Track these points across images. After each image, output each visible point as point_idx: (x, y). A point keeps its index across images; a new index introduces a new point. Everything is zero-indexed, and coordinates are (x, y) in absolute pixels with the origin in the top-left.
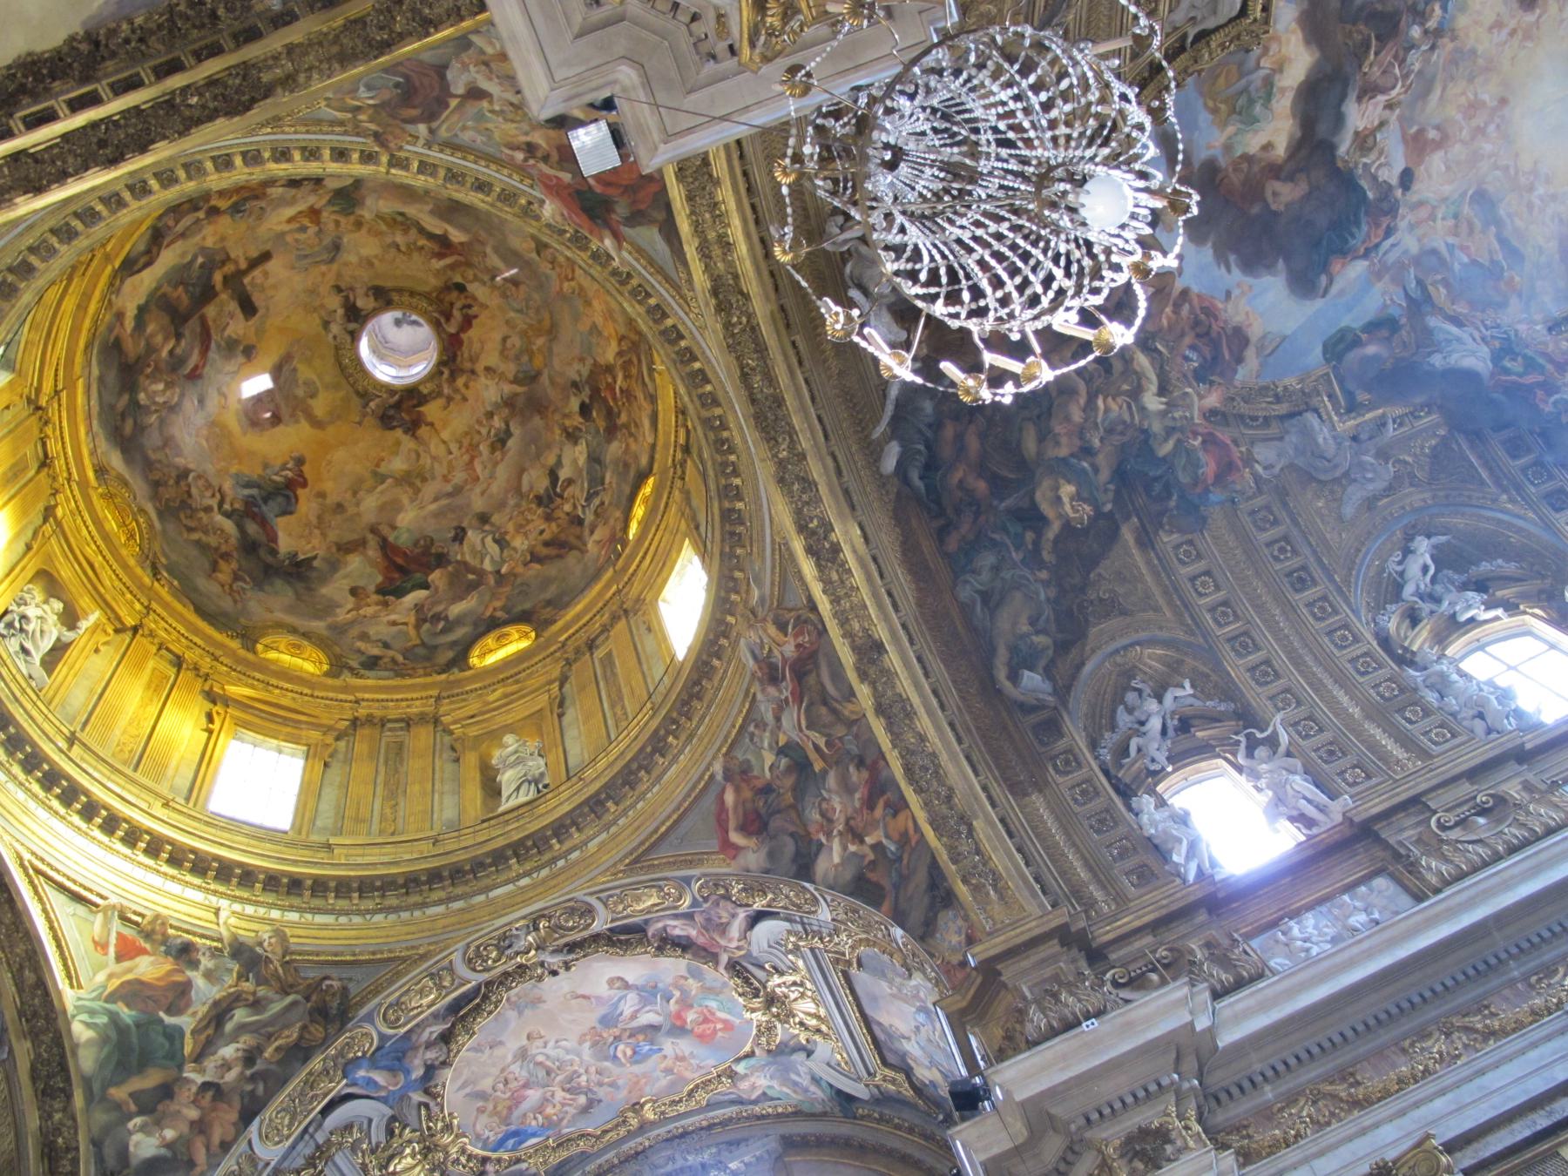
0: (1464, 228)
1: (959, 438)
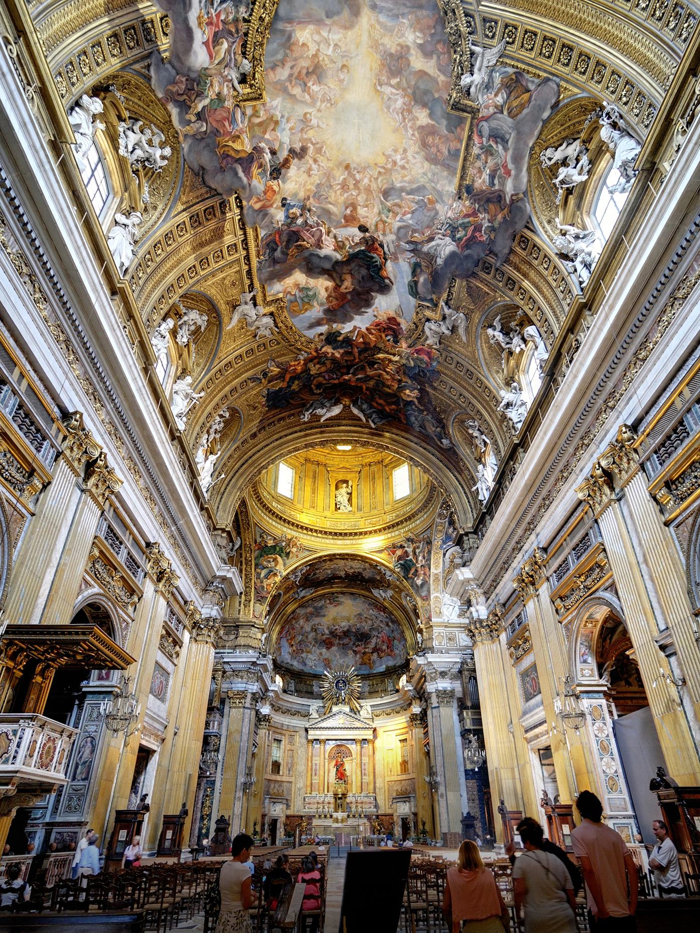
0: (396, 209)
1: (377, 403)
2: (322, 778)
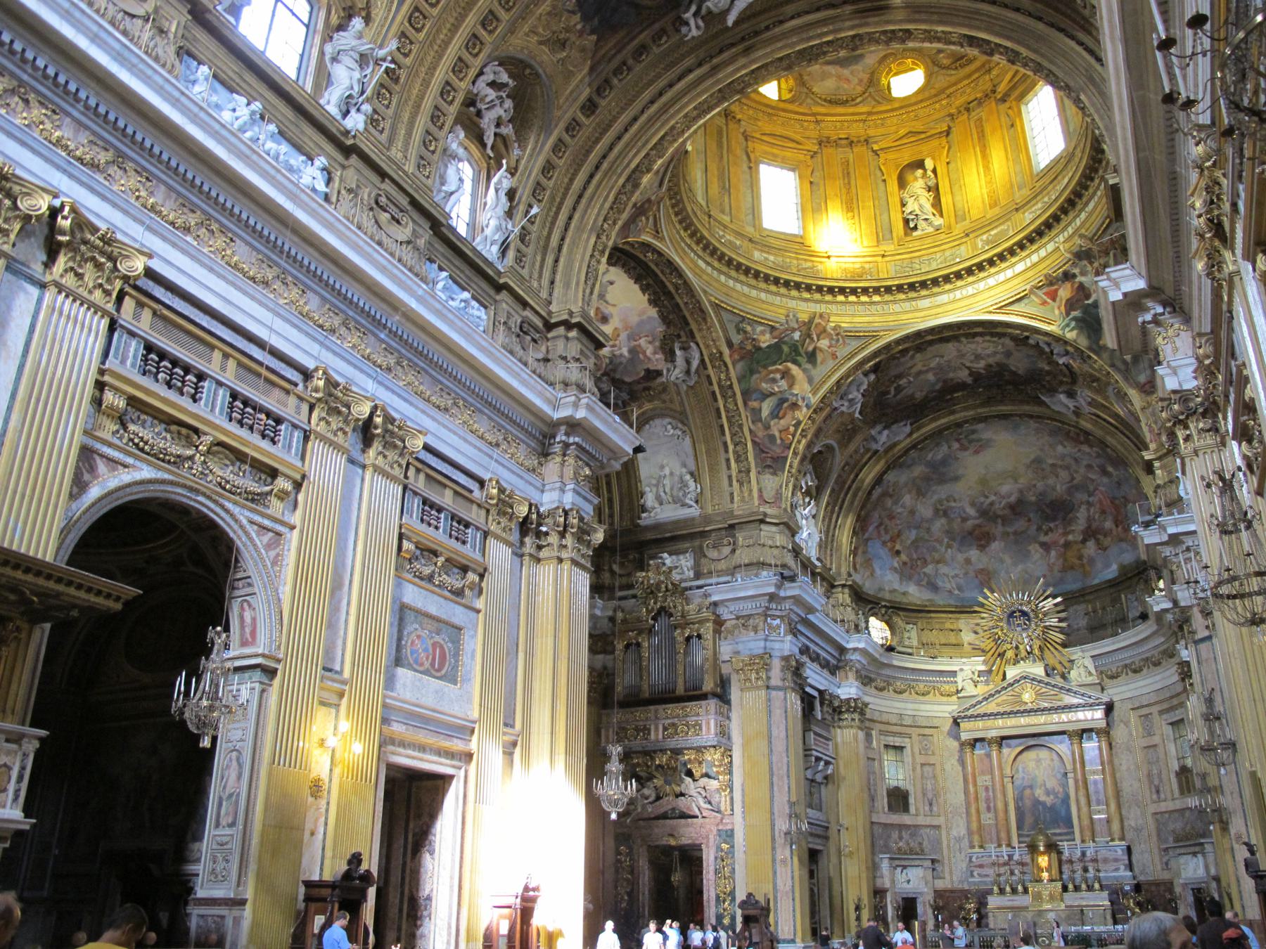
2: (1001, 815)
